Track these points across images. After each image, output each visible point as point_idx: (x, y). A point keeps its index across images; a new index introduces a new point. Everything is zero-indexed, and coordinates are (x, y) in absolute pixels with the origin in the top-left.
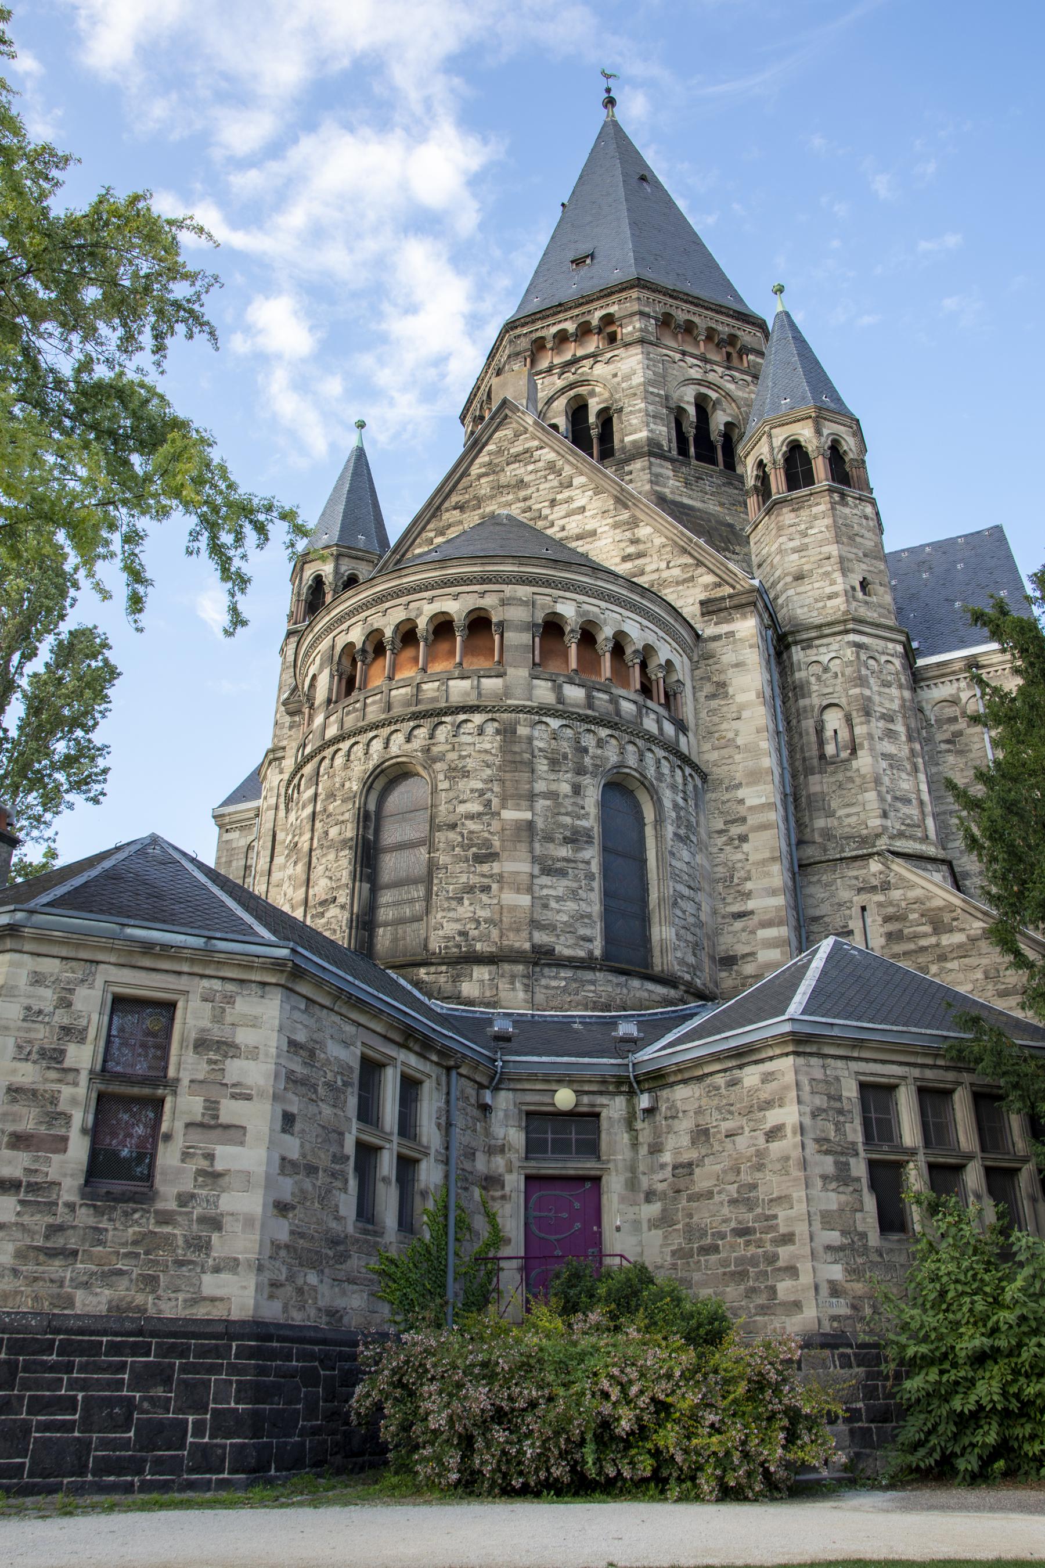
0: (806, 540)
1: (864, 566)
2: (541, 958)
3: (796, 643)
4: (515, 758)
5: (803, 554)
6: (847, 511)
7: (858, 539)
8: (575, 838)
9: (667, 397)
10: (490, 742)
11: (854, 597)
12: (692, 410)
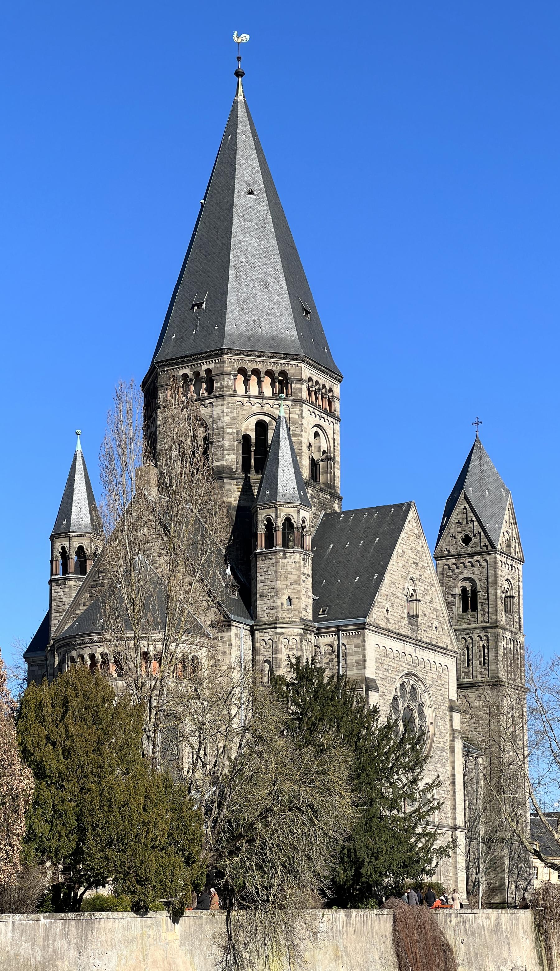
0: (266, 577)
1: (289, 591)
3: (257, 630)
5: (265, 584)
6: (285, 561)
7: (289, 576)
9: (238, 433)
11: (282, 608)
12: (253, 435)
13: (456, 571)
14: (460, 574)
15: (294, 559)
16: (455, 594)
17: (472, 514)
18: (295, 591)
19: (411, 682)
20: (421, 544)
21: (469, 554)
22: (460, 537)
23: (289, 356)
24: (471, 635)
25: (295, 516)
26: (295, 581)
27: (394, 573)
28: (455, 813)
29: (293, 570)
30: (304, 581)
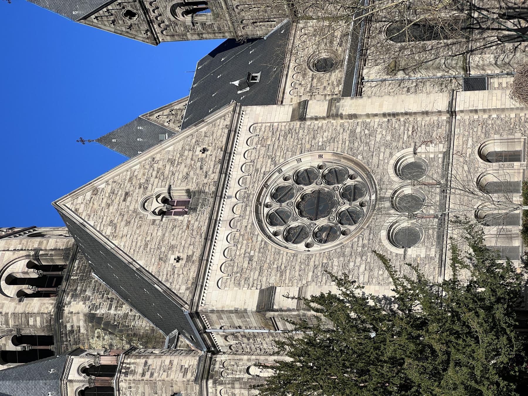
13: (167, 23)
14: (169, 19)
15: (126, 389)
16: (193, 23)
17: (101, 12)
18: (164, 389)
19: (268, 200)
20: (103, 186)
21: (145, 13)
24: (235, 7)
25: (76, 386)
26: (152, 388)
27: (134, 244)
28: (432, 113)
29: (140, 391)
30: (152, 375)
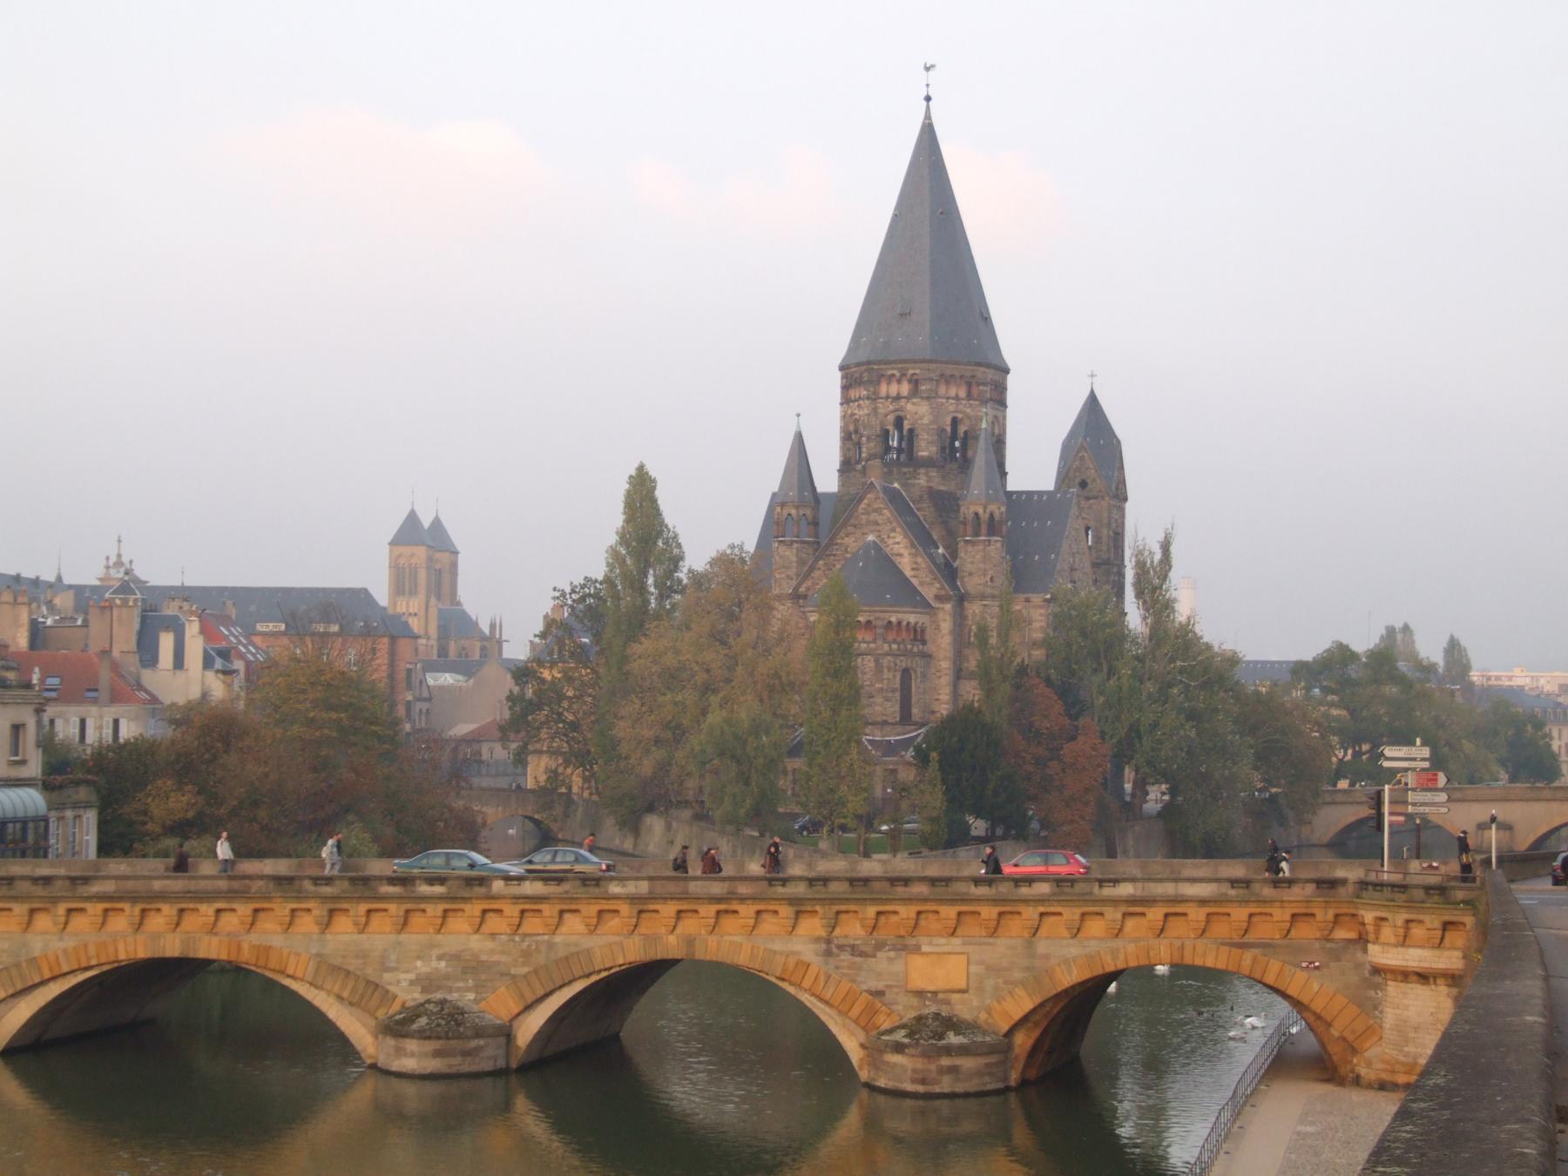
2: (885, 723)
4: (879, 669)
8: (893, 691)
10: (872, 664)
12: (949, 429)
22: (1078, 480)
23: (980, 364)
